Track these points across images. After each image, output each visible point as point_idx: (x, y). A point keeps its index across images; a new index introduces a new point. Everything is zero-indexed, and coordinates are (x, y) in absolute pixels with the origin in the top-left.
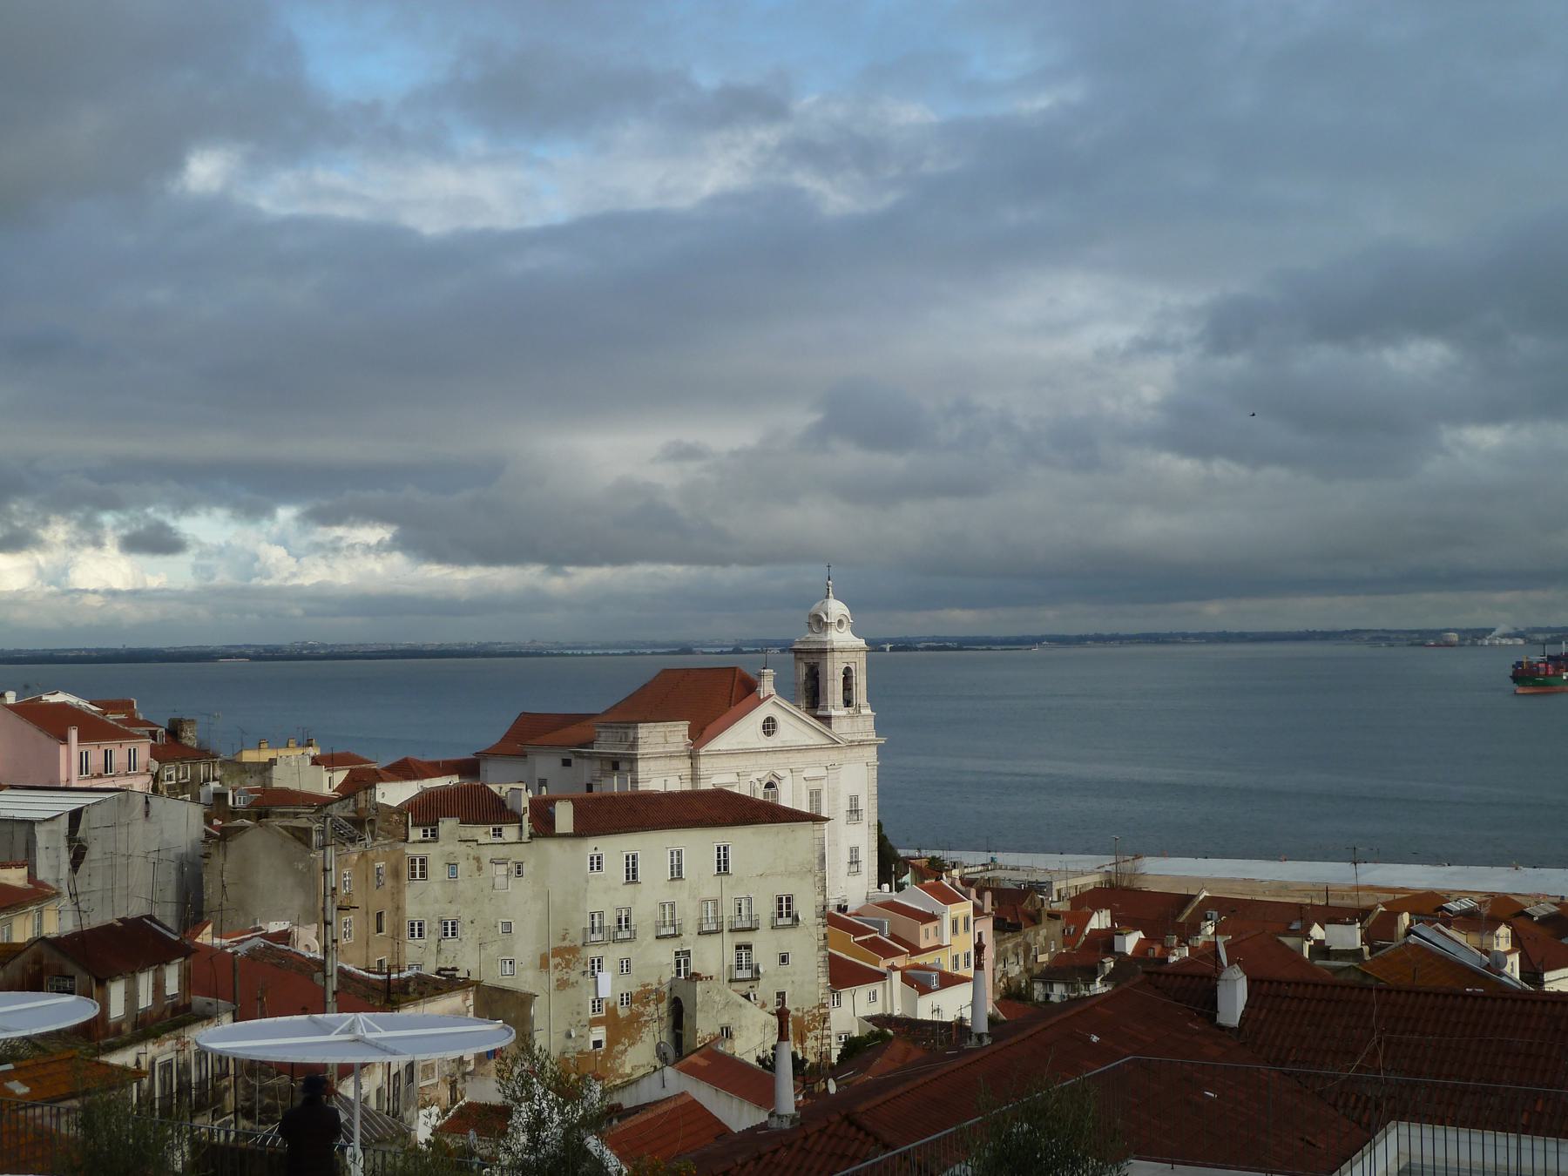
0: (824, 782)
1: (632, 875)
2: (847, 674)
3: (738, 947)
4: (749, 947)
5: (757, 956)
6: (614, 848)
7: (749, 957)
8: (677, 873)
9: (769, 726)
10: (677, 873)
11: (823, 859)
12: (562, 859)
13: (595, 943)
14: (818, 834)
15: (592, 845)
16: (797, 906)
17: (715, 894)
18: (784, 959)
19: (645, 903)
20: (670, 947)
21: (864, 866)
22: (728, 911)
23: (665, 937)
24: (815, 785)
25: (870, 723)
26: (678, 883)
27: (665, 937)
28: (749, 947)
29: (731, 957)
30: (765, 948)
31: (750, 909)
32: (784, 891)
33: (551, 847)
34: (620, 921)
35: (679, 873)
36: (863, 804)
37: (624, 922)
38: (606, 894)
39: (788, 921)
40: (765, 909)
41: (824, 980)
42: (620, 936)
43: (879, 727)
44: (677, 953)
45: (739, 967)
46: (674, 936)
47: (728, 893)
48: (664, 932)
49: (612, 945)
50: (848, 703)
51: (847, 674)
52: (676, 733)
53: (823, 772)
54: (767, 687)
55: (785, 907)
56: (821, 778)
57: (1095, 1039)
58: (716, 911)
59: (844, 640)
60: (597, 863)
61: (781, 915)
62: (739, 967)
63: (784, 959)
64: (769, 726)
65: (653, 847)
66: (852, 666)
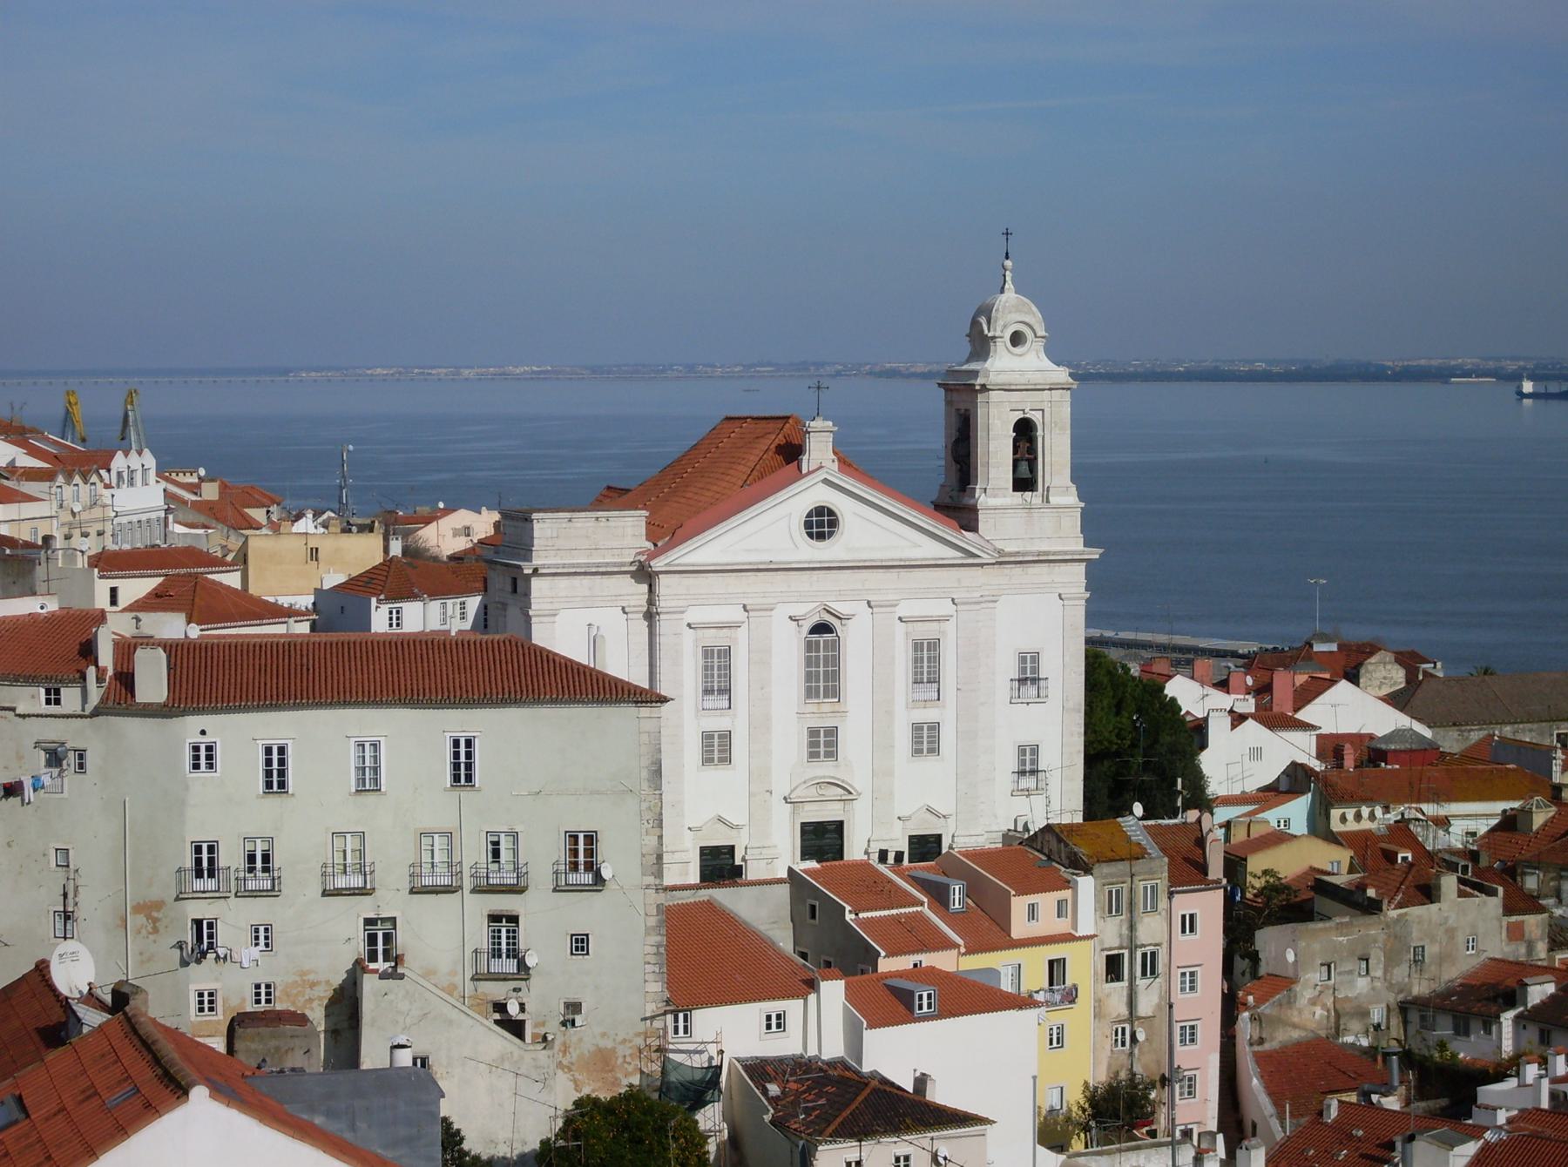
0: (949, 627)
1: (276, 777)
2: (1025, 431)
3: (495, 918)
4: (514, 919)
5: (526, 935)
6: (240, 735)
7: (513, 936)
8: (369, 780)
9: (821, 524)
10: (369, 780)
11: (657, 772)
12: (149, 745)
13: (202, 895)
14: (647, 726)
15: (190, 728)
16: (604, 850)
17: (447, 822)
18: (580, 944)
19: (303, 830)
20: (365, 908)
21: (1054, 781)
22: (474, 854)
23: (338, 893)
24: (925, 632)
25: (1073, 522)
26: (371, 799)
27: (338, 893)
28: (514, 919)
29: (480, 936)
30: (544, 920)
31: (515, 852)
32: (582, 825)
33: (133, 728)
34: (251, 858)
35: (376, 781)
36: (1049, 667)
37: (261, 861)
38: (227, 808)
39: (588, 878)
40: (542, 854)
41: (656, 987)
42: (251, 885)
43: (1092, 529)
44: (369, 922)
45: (496, 953)
46: (363, 892)
47: (474, 819)
48: (341, 882)
49: (233, 901)
50: (1024, 483)
51: (1025, 431)
52: (626, 532)
53: (946, 608)
54: (820, 449)
55: (583, 854)
56: (735, 626)
57: (1361, 1133)
58: (450, 853)
59: (1023, 376)
60: (204, 757)
61: (574, 867)
62: (496, 953)
63: (580, 944)
64: (821, 524)
65: (321, 737)
66: (1036, 417)
